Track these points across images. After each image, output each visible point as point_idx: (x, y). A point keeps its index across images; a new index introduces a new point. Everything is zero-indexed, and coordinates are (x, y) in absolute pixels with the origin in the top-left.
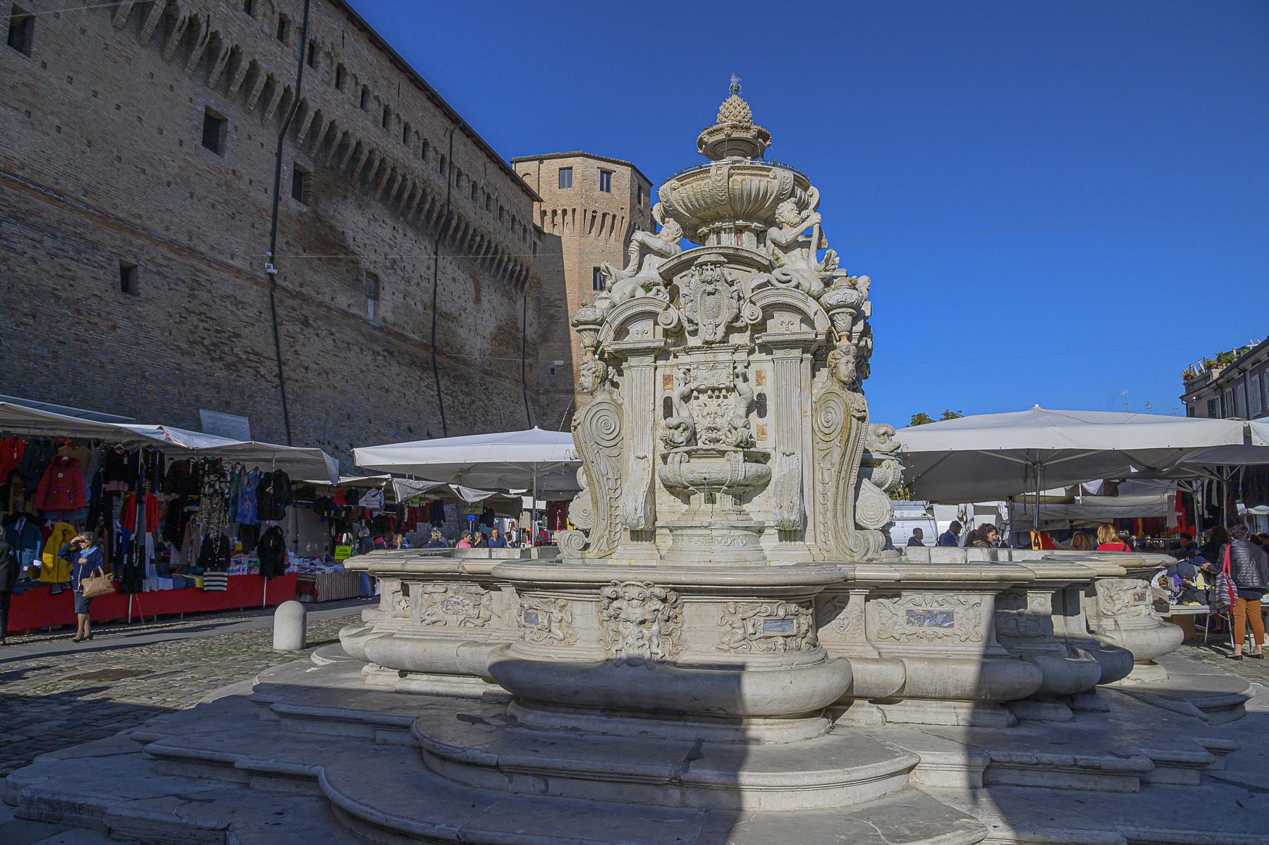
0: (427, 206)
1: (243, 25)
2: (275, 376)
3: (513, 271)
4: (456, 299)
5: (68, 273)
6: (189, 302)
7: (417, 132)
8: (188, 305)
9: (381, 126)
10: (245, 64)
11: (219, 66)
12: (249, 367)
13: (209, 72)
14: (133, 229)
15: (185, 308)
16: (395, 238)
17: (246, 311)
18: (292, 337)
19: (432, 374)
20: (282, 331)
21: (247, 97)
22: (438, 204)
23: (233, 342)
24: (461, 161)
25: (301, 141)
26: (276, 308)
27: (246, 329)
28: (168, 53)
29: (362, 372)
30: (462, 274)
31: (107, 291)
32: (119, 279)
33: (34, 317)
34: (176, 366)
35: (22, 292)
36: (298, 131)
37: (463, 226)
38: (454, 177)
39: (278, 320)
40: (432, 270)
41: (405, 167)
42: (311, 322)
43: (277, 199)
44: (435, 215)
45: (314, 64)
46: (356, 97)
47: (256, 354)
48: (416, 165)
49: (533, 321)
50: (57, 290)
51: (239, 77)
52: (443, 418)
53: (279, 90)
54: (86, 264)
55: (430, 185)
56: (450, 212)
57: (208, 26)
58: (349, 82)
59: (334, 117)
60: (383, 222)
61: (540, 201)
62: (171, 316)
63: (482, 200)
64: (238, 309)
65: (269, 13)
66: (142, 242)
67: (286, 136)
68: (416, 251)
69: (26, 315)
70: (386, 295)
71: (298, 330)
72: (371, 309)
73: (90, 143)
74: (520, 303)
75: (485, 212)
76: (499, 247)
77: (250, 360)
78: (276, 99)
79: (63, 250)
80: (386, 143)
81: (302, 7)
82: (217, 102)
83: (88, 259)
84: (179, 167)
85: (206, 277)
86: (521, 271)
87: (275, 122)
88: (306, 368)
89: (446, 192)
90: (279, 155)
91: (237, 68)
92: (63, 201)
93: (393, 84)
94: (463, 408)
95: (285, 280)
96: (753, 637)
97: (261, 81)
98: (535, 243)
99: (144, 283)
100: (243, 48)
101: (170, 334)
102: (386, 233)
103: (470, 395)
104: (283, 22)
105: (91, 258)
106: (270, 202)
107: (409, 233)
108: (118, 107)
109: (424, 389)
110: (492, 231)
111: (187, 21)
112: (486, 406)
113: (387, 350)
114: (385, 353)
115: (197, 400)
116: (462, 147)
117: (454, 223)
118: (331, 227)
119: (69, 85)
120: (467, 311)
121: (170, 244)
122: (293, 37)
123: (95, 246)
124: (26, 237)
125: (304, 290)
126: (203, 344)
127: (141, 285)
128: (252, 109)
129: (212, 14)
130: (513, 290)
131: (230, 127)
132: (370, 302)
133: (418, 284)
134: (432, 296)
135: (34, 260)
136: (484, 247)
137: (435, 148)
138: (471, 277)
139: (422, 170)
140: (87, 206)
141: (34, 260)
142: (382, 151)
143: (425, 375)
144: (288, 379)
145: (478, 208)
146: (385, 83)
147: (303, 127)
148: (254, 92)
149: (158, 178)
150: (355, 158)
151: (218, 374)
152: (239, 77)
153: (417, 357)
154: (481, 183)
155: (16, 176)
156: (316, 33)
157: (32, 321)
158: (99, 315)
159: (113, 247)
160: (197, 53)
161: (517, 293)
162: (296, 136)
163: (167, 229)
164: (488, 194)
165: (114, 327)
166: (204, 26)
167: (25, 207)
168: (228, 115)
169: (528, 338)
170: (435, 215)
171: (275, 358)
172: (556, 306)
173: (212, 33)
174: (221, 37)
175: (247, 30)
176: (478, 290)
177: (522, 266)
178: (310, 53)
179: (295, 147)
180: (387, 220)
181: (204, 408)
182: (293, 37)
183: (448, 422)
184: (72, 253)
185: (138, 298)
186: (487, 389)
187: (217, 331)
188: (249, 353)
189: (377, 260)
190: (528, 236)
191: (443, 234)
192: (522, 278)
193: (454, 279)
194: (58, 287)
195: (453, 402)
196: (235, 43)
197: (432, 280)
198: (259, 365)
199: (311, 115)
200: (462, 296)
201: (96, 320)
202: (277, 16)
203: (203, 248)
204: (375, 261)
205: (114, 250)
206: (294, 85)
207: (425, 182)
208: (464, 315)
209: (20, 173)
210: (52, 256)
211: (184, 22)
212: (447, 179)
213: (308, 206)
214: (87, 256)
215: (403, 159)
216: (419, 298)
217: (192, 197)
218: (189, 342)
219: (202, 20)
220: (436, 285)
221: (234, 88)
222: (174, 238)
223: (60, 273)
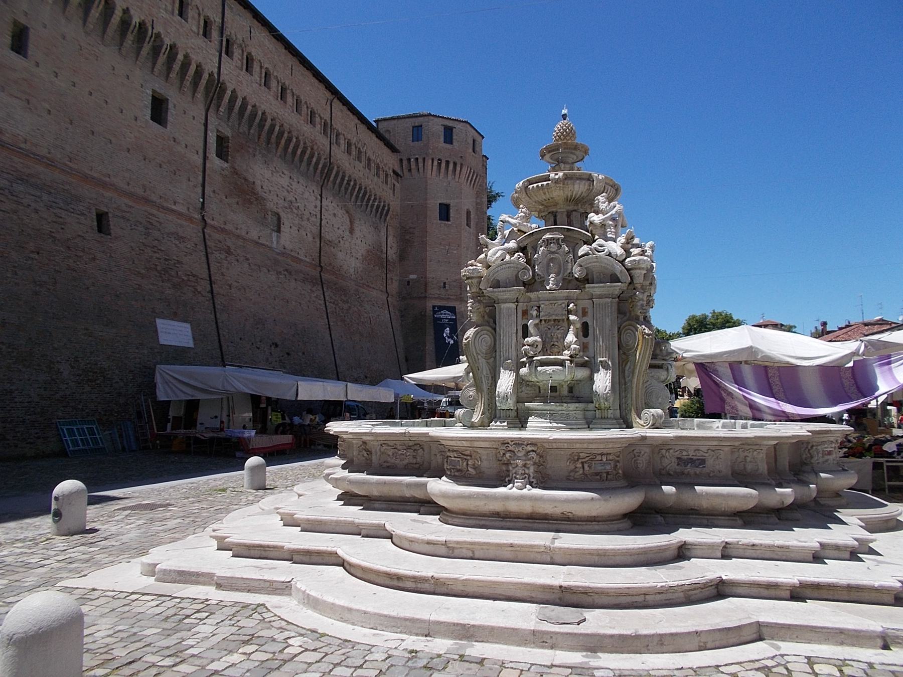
0: (314, 160)
1: (178, 27)
2: (208, 292)
3: (378, 207)
5: (60, 220)
6: (145, 238)
7: (306, 103)
8: (144, 241)
9: (279, 99)
11: (162, 58)
12: (189, 286)
13: (154, 64)
14: (105, 185)
15: (143, 243)
16: (291, 185)
17: (186, 244)
18: (219, 263)
19: (320, 287)
20: (211, 257)
22: (323, 158)
23: (177, 267)
25: (221, 114)
26: (207, 241)
27: (186, 258)
28: (124, 51)
29: (269, 287)
30: (340, 211)
31: (87, 232)
32: (95, 223)
33: (38, 253)
34: (137, 286)
36: (219, 107)
37: (341, 173)
39: (209, 250)
41: (298, 131)
42: (232, 251)
43: (205, 158)
44: (320, 166)
45: (229, 54)
46: (261, 78)
47: (194, 276)
48: (306, 129)
49: (394, 245)
50: (53, 232)
51: (177, 67)
52: (328, 322)
53: (206, 76)
54: (72, 212)
55: (316, 143)
57: (153, 28)
58: (256, 67)
59: (245, 94)
60: (283, 173)
62: (133, 250)
63: (354, 153)
64: (180, 243)
65: (196, 16)
66: (111, 195)
67: (211, 110)
68: (307, 195)
70: (285, 228)
71: (223, 257)
72: (274, 239)
75: (357, 162)
76: (368, 188)
77: (190, 281)
78: (203, 82)
80: (283, 112)
83: (73, 209)
84: (136, 137)
85: (156, 219)
86: (384, 206)
87: (202, 99)
88: (230, 286)
89: (329, 149)
90: (206, 125)
92: (54, 166)
93: (287, 66)
94: (343, 312)
95: (213, 220)
97: (193, 68)
98: (394, 185)
99: (114, 224)
100: (179, 44)
101: (133, 263)
102: (284, 181)
103: (348, 302)
104: (207, 24)
105: (75, 207)
106: (201, 161)
107: (302, 181)
108: (91, 94)
109: (314, 299)
112: (359, 310)
113: (286, 270)
114: (286, 273)
115: (153, 312)
116: (339, 114)
118: (246, 180)
119: (56, 79)
120: (344, 239)
121: (131, 195)
122: (215, 34)
124: (30, 194)
125: (226, 227)
126: (156, 269)
127: (112, 227)
128: (185, 90)
129: (155, 19)
131: (170, 106)
132: (274, 234)
133: (308, 219)
134: (319, 228)
135: (36, 211)
136: (357, 189)
137: (319, 116)
138: (347, 212)
139: (310, 133)
140: (71, 168)
141: (36, 211)
143: (314, 289)
144: (217, 294)
145: (352, 160)
146: (282, 66)
147: (223, 103)
148: (187, 77)
150: (261, 126)
151: (168, 292)
152: (177, 67)
153: (308, 275)
154: (354, 140)
155: (21, 148)
157: (36, 256)
158: (83, 251)
159: (90, 199)
162: (218, 110)
163: (128, 184)
165: (94, 259)
168: (168, 96)
169: (389, 258)
170: (320, 166)
171: (208, 279)
172: (410, 233)
173: (155, 34)
174: (163, 36)
175: (181, 30)
176: (352, 223)
177: (384, 202)
178: (227, 48)
179: (217, 118)
181: (158, 317)
182: (215, 34)
185: (109, 237)
186: (359, 298)
187: (166, 260)
188: (189, 275)
190: (389, 179)
193: (335, 215)
194: (54, 231)
195: (335, 308)
196: (173, 40)
197: (319, 217)
198: (196, 284)
199: (229, 92)
200: (341, 227)
201: (81, 254)
202: (202, 18)
203: (154, 198)
204: (277, 203)
205: (91, 202)
206: (216, 70)
207: (312, 141)
209: (23, 146)
210: (49, 207)
211: (135, 26)
212: (329, 139)
213: (228, 162)
214: (72, 206)
215: (296, 124)
216: (309, 230)
217: (145, 160)
218: (146, 268)
220: (321, 220)
221: (173, 75)
222: (133, 190)
223: (54, 220)
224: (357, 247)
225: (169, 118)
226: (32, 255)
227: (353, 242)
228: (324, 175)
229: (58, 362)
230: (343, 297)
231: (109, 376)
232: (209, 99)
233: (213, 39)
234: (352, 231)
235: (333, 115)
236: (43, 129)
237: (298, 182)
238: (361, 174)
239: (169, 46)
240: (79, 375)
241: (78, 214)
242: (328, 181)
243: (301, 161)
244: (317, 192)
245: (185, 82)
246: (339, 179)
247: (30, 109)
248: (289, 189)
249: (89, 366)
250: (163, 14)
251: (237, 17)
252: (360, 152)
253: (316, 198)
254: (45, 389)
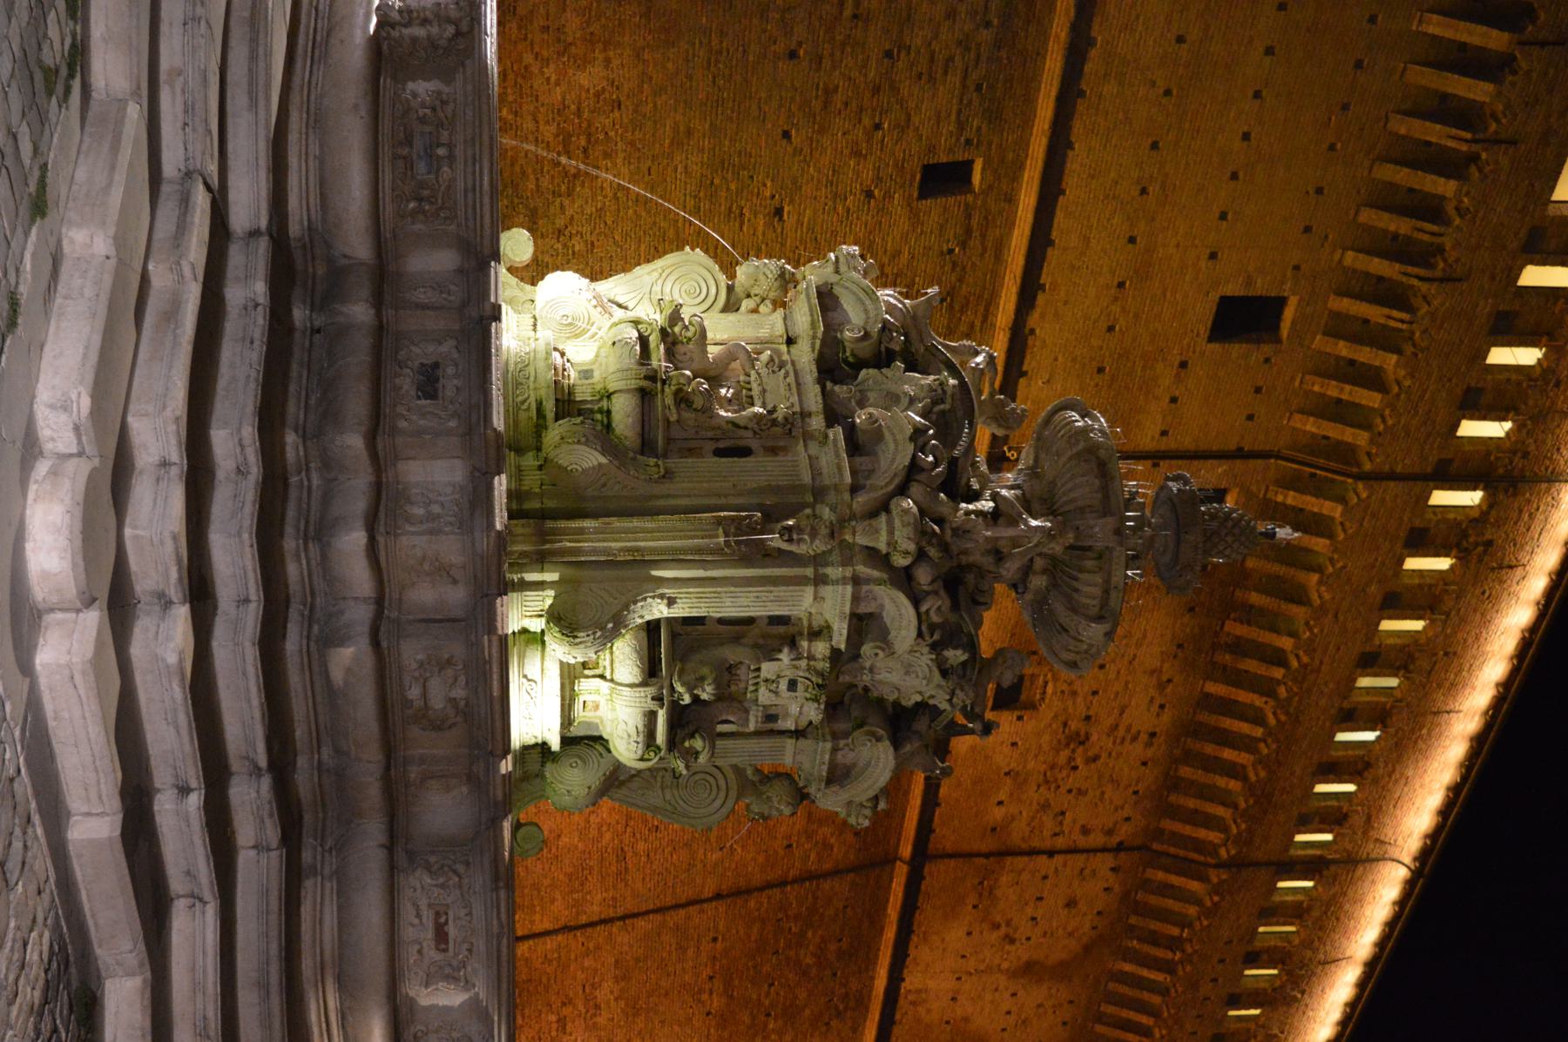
16: (1135, 739)
28: (1368, 216)
30: (1088, 925)
33: (855, 16)
40: (1082, 842)
50: (909, 53)
54: (961, 100)
60: (1162, 707)
85: (978, 324)
90: (1240, 454)
102: (1141, 716)
108: (1246, 137)
135: (951, 14)
138: (1087, 949)
141: (951, 14)
147: (1308, 498)
148: (1348, 387)
157: (848, 12)
165: (857, 154)
170: (1202, 833)
176: (1061, 972)
180: (1166, 717)
183: (752, 904)
185: (916, 194)
189: (1079, 700)
193: (1071, 904)
194: (913, 55)
197: (1060, 842)
201: (867, 121)
204: (1074, 693)
208: (994, 936)
210: (964, 43)
220: (1051, 853)
224: (988, 996)
227: (1003, 981)
229: (608, 61)
230: (833, 947)
232: (1308, 458)
236: (1140, 28)
237: (1144, 764)
240: (579, 113)
241: (959, 113)
244: (1124, 832)
245: (1334, 383)
248: (1121, 732)
253: (1110, 832)
254: (545, 29)
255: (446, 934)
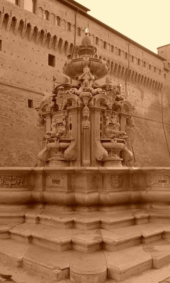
4: (134, 97)
7: (116, 47)
9: (103, 48)
10: (58, 39)
11: (51, 42)
13: (49, 44)
21: (60, 49)
24: (133, 53)
32: (28, 104)
35: (3, 110)
38: (131, 59)
50: (11, 108)
51: (57, 43)
53: (69, 45)
56: (130, 71)
57: (46, 32)
61: (165, 60)
63: (142, 64)
65: (64, 23)
69: (4, 115)
73: (18, 70)
74: (160, 95)
75: (143, 68)
76: (150, 78)
78: (69, 47)
79: (13, 98)
80: (105, 53)
81: (74, 19)
82: (52, 52)
91: (56, 41)
96: (3, 184)
100: (57, 36)
110: (147, 73)
111: (40, 32)
112: (147, 130)
117: (132, 74)
122: (72, 28)
123: (21, 96)
129: (47, 28)
130: (157, 91)
131: (56, 58)
138: (140, 89)
141: (6, 102)
142: (104, 56)
148: (62, 47)
149: (37, 76)
152: (57, 43)
156: (79, 25)
157: (5, 117)
158: (23, 114)
160: (45, 39)
161: (158, 92)
164: (144, 62)
165: (27, 117)
166: (45, 32)
167: (3, 89)
174: (50, 34)
182: (72, 28)
184: (15, 99)
185: (33, 109)
186: (147, 124)
191: (128, 78)
192: (160, 87)
193: (133, 91)
205: (26, 97)
207: (120, 63)
210: (10, 100)
212: (128, 61)
219: (45, 30)
221: (56, 47)
225: (56, 63)
226: (4, 117)
227: (143, 101)
228: (127, 75)
229: (12, 152)
230: (138, 125)
231: (31, 157)
233: (72, 30)
234: (142, 97)
235: (130, 50)
238: (146, 72)
239: (53, 37)
240: (20, 157)
241: (21, 102)
242: (129, 78)
243: (115, 71)
246: (134, 76)
247: (3, 68)
249: (23, 154)
250: (50, 26)
251: (82, 20)
252: (145, 62)
253: (124, 86)
254: (7, 161)
255: (164, 180)
